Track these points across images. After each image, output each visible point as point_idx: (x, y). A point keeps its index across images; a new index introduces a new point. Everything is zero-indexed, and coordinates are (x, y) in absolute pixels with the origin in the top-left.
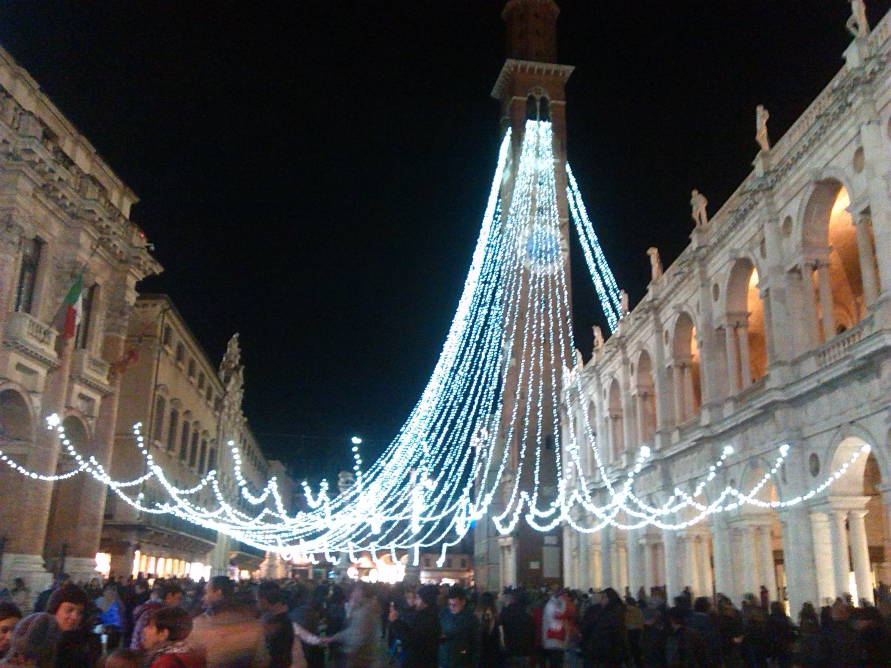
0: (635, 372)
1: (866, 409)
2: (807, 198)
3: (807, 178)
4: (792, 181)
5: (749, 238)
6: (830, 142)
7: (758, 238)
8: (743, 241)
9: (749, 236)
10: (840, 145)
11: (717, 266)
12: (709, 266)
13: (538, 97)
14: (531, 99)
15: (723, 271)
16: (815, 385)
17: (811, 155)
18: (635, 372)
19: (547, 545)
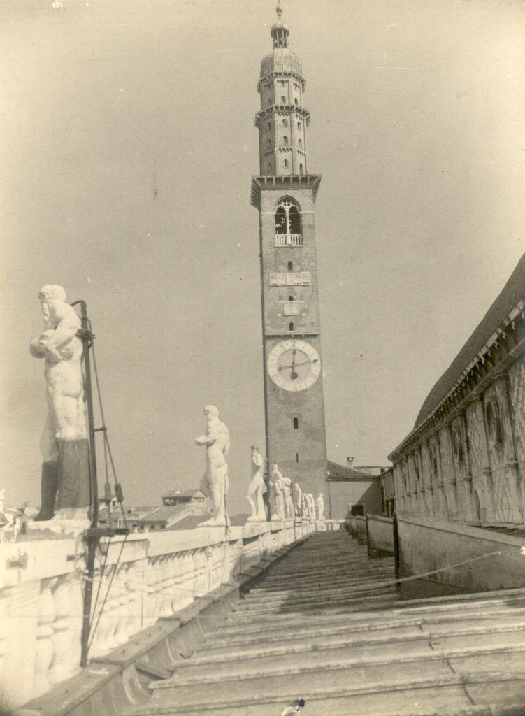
13: (287, 209)
14: (281, 210)
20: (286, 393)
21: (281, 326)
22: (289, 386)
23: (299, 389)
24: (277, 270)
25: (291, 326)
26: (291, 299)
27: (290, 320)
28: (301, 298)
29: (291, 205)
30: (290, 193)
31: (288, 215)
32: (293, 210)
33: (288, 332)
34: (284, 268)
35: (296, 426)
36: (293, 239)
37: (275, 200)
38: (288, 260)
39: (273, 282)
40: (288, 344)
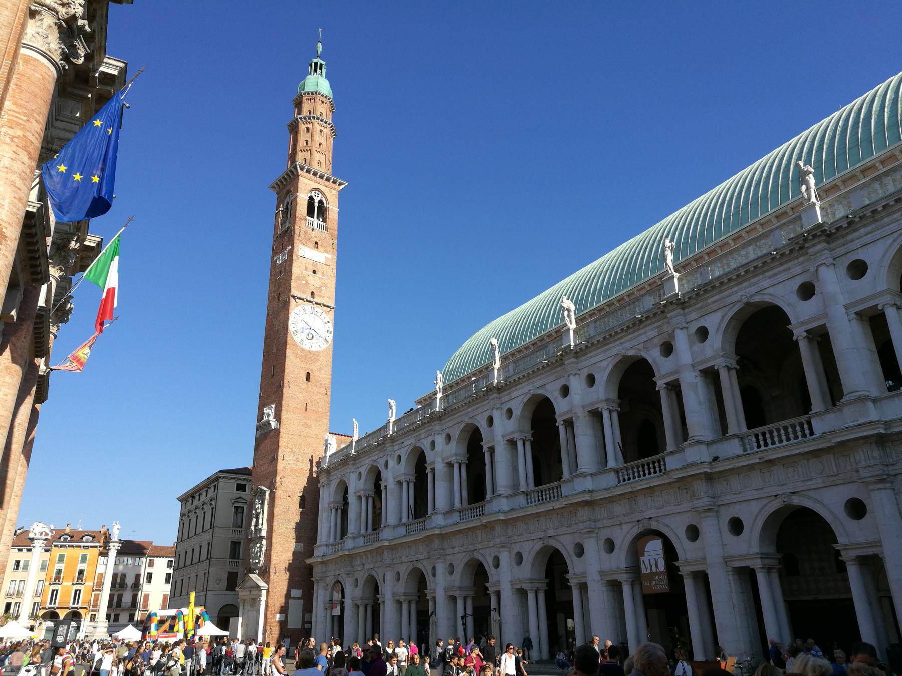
0: (453, 443)
1: (819, 482)
2: (731, 314)
3: (734, 298)
4: (710, 301)
5: (645, 339)
6: (767, 274)
7: (658, 341)
8: (635, 342)
9: (643, 338)
10: (780, 278)
11: (594, 360)
12: (583, 358)
13: (316, 200)
14: (311, 198)
15: (604, 363)
16: (758, 460)
17: (741, 283)
18: (453, 443)
19: (294, 598)
20: (302, 350)
21: (304, 292)
22: (306, 345)
23: (314, 349)
24: (305, 244)
25: (313, 294)
26: (314, 272)
27: (312, 289)
28: (323, 274)
29: (320, 197)
30: (322, 188)
31: (316, 205)
32: (320, 202)
33: (310, 299)
34: (312, 245)
35: (308, 379)
36: (319, 226)
37: (310, 188)
38: (315, 240)
39: (300, 253)
40: (308, 306)
